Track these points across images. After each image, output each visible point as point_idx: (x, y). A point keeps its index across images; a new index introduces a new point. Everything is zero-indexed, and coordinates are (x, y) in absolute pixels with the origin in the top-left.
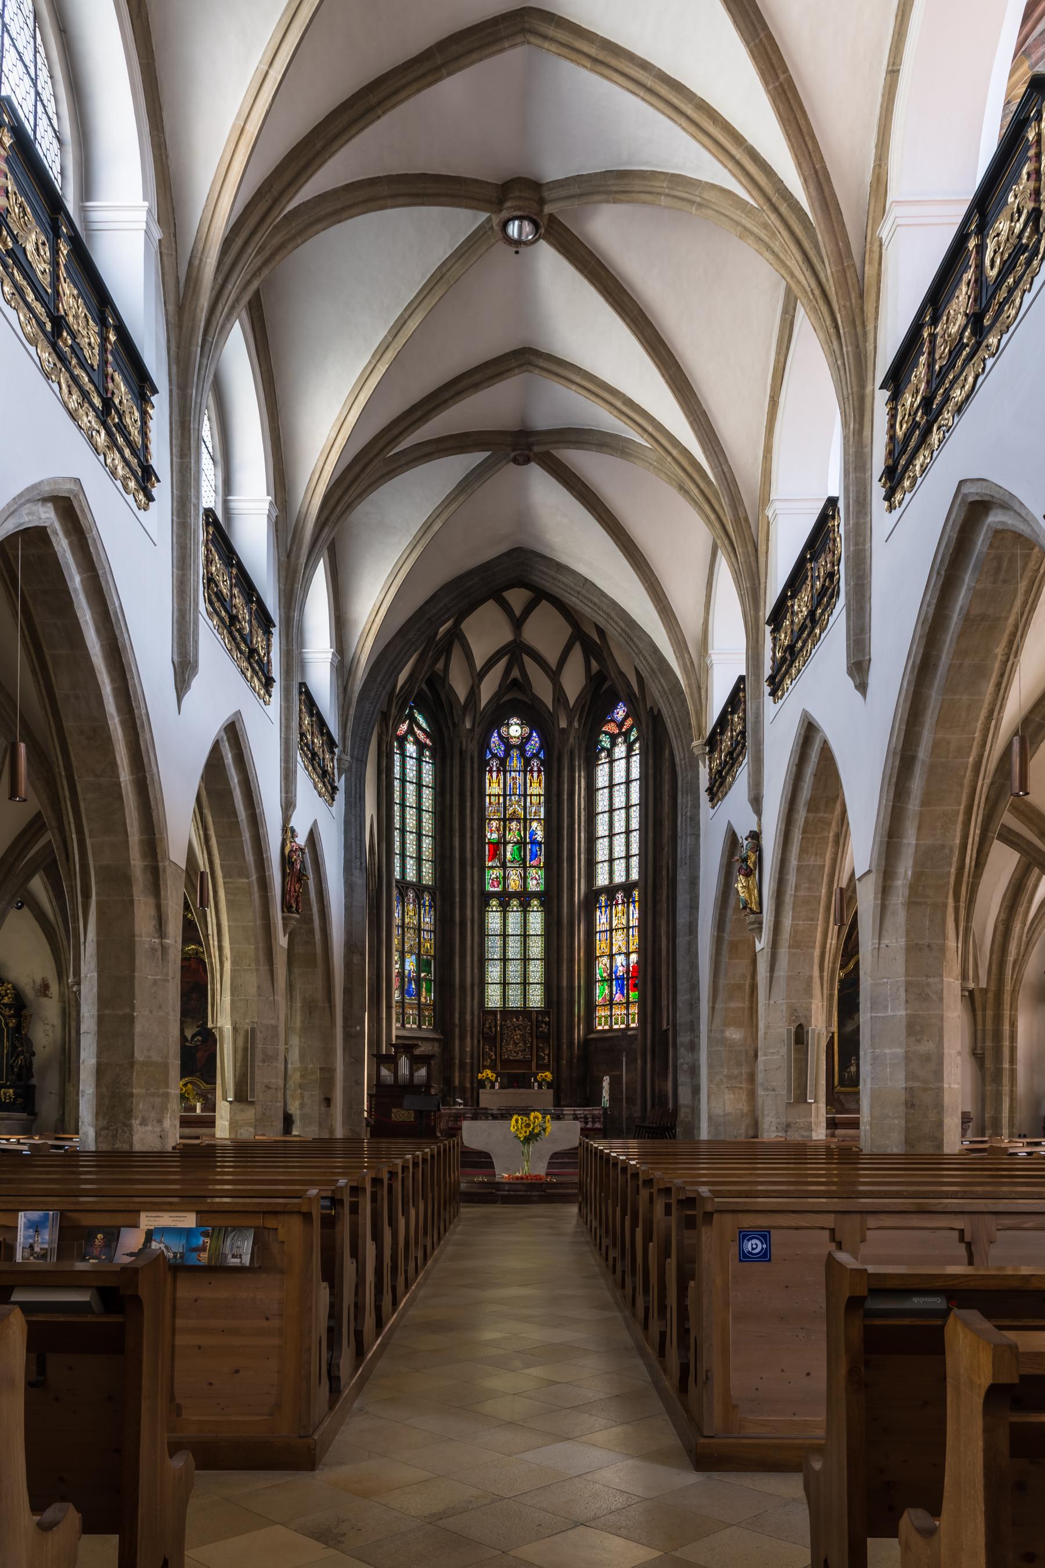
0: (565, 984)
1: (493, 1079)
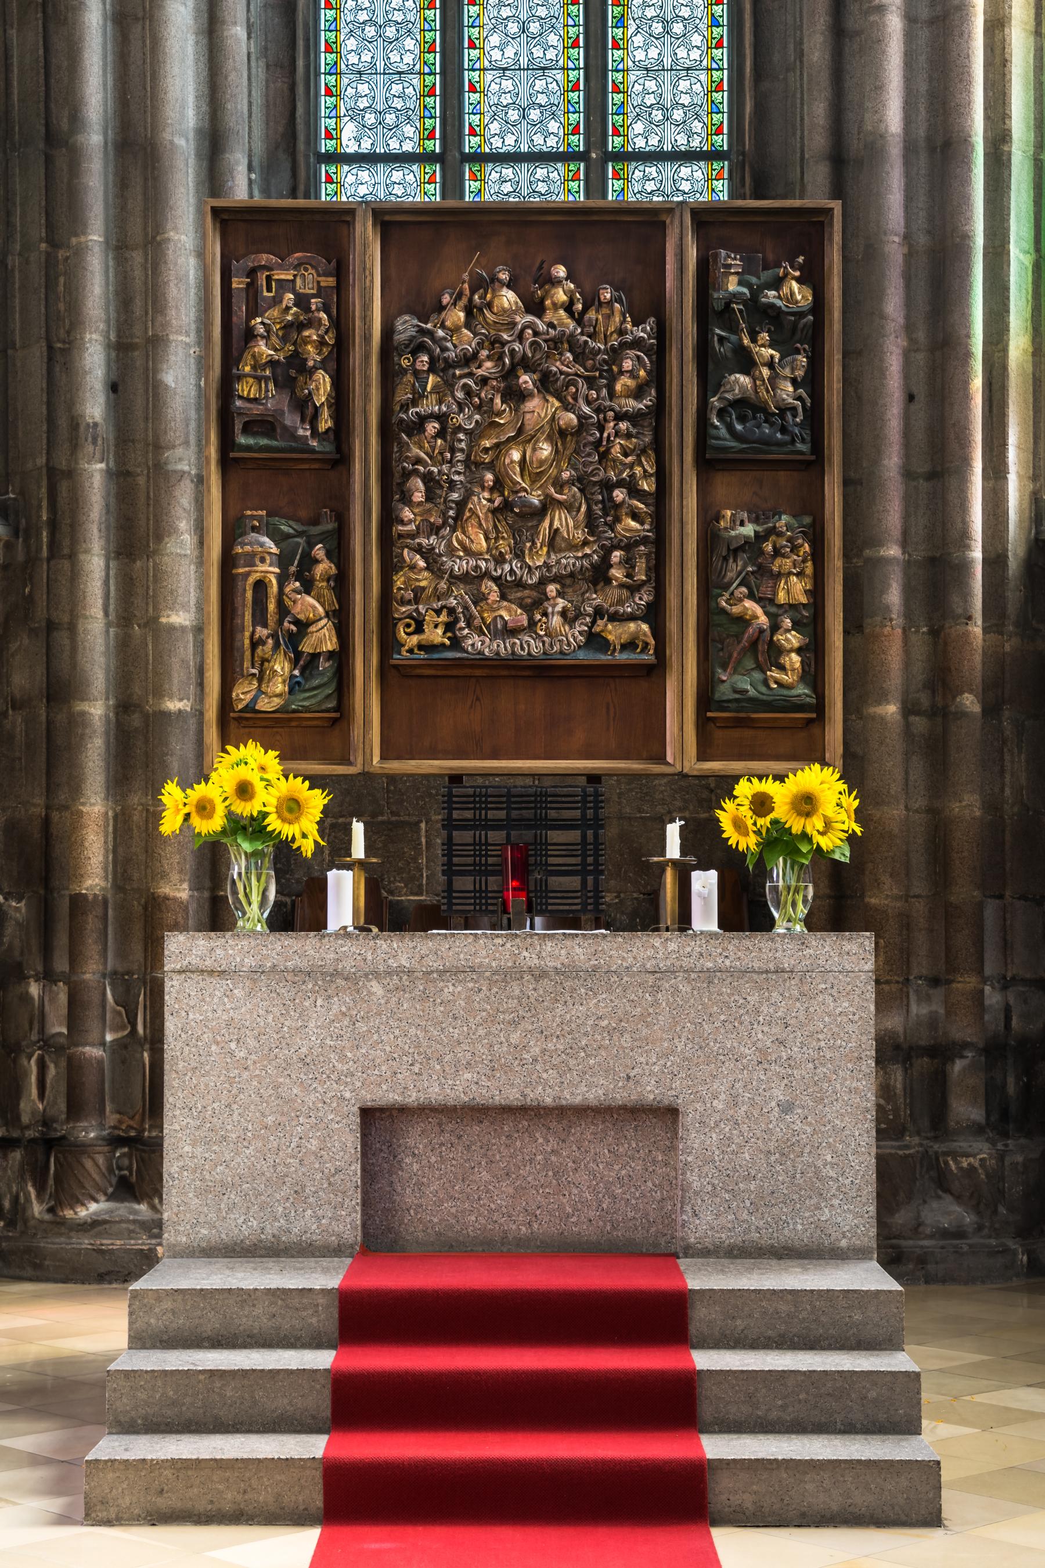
0: (893, 116)
1: (305, 833)
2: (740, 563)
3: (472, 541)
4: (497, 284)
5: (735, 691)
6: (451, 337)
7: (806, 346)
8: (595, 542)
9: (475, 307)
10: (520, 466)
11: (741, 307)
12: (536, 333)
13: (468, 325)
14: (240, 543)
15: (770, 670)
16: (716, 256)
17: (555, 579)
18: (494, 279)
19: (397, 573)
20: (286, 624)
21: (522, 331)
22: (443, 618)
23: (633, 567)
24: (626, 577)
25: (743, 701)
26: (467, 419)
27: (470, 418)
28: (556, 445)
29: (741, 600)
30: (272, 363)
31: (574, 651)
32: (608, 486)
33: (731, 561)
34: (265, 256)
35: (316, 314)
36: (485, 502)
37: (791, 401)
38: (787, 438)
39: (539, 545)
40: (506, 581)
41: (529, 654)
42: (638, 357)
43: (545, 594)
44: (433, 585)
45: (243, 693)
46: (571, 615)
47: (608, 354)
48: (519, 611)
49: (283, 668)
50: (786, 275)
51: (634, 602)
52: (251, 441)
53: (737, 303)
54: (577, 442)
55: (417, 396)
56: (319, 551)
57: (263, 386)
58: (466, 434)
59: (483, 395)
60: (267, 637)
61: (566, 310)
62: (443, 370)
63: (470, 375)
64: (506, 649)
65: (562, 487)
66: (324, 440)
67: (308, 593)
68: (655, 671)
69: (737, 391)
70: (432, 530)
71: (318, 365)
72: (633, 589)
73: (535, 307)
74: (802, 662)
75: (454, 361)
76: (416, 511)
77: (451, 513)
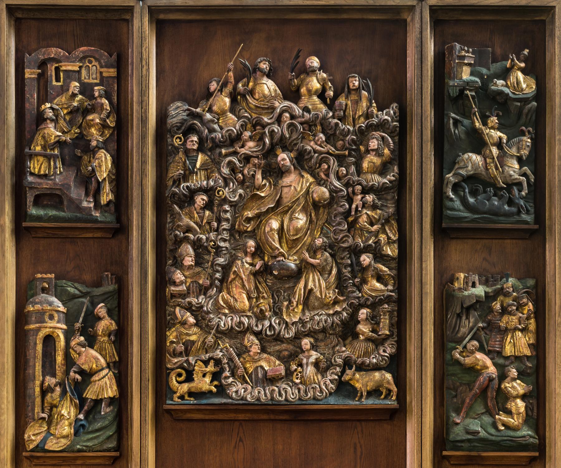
2: (472, 320)
3: (236, 300)
4: (258, 73)
5: (468, 432)
6: (218, 119)
7: (531, 129)
8: (344, 301)
9: (239, 94)
10: (278, 234)
11: (474, 94)
12: (293, 117)
13: (232, 110)
14: (32, 303)
15: (498, 414)
16: (452, 49)
17: (309, 334)
18: (256, 69)
19: (170, 329)
20: (72, 374)
21: (280, 115)
22: (211, 368)
23: (378, 324)
24: (372, 332)
25: (475, 441)
26: (232, 193)
27: (234, 191)
28: (311, 215)
29: (472, 352)
30: (60, 143)
31: (326, 397)
32: (356, 252)
33: (464, 318)
34: (54, 50)
35: (99, 100)
36: (247, 266)
37: (517, 176)
38: (514, 209)
39: (295, 303)
40: (266, 335)
41: (286, 400)
42: (383, 138)
43: (300, 347)
44: (201, 340)
45: (34, 435)
46: (322, 365)
47: (356, 135)
48: (278, 362)
49: (69, 413)
50: (512, 67)
51: (379, 354)
52: (41, 212)
53: (470, 91)
54: (329, 214)
55: (187, 172)
56: (101, 309)
57: (52, 163)
58: (231, 206)
59: (246, 172)
60: (56, 386)
61: (319, 97)
62: (211, 150)
63: (235, 153)
64: (266, 396)
65: (315, 252)
66: (106, 211)
67: (92, 347)
68: (397, 415)
69: (470, 168)
70: (200, 290)
71: (101, 145)
72: (378, 342)
73: (292, 94)
74: (526, 407)
75: (220, 141)
76: (187, 273)
77: (218, 275)
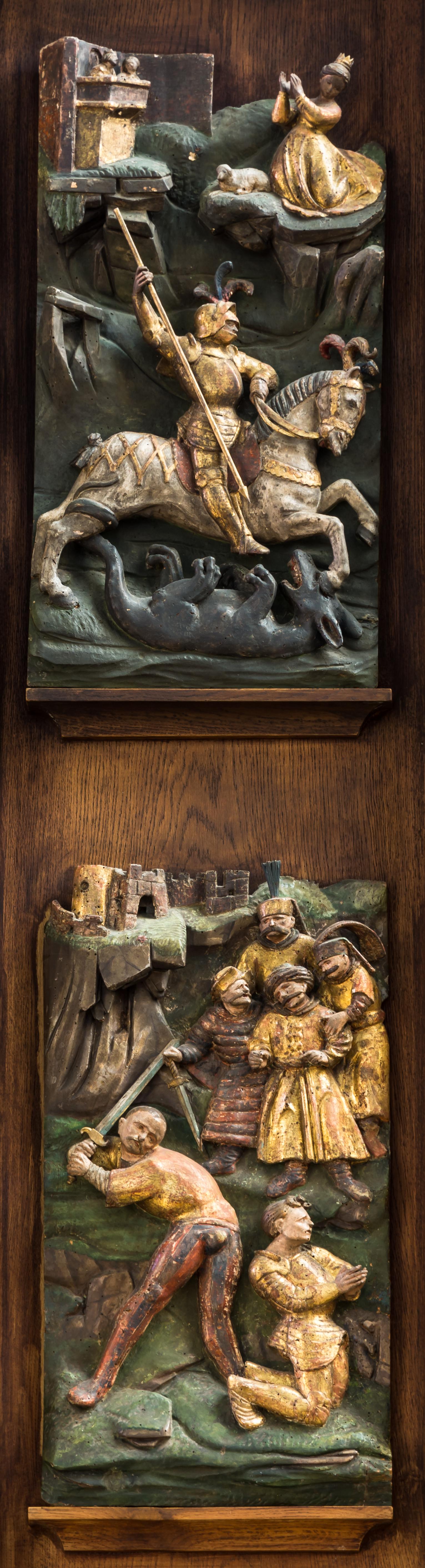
2: (142, 1034)
15: (241, 1372)
33: (112, 1025)
